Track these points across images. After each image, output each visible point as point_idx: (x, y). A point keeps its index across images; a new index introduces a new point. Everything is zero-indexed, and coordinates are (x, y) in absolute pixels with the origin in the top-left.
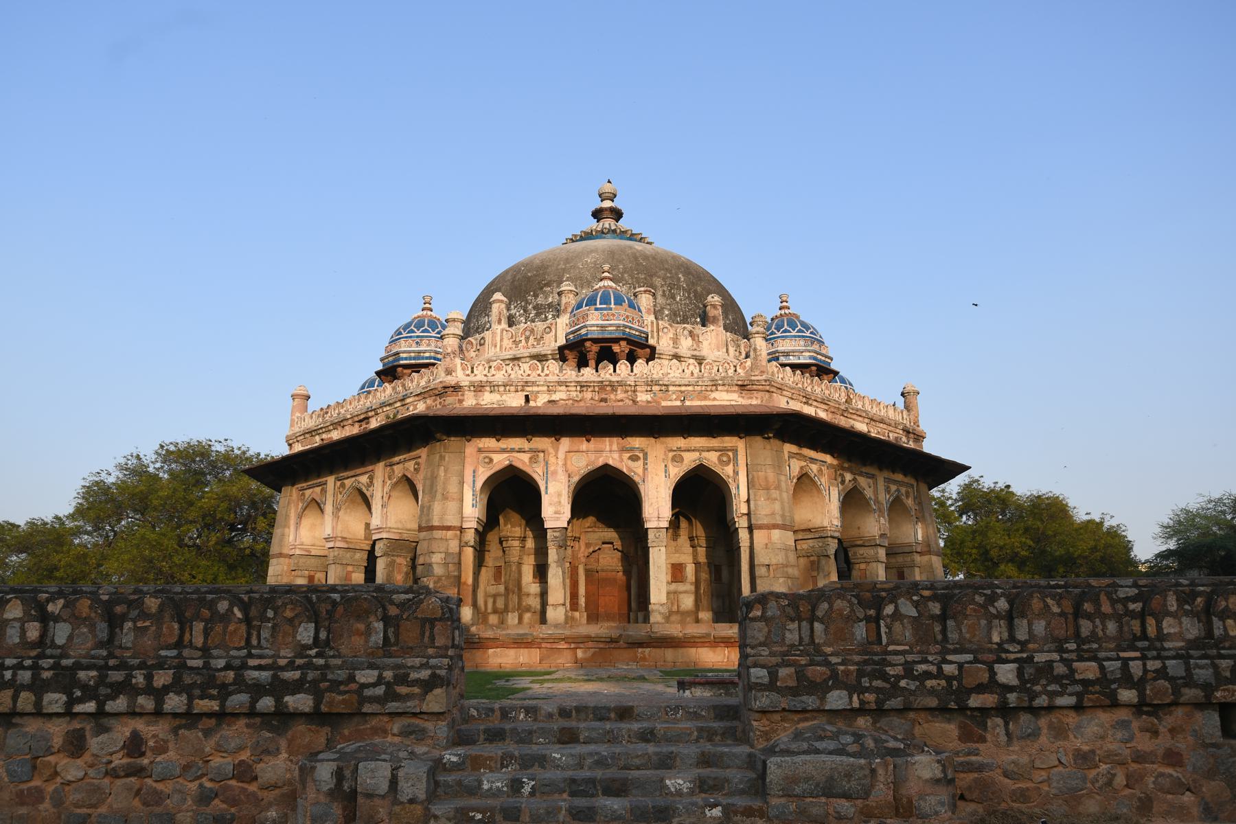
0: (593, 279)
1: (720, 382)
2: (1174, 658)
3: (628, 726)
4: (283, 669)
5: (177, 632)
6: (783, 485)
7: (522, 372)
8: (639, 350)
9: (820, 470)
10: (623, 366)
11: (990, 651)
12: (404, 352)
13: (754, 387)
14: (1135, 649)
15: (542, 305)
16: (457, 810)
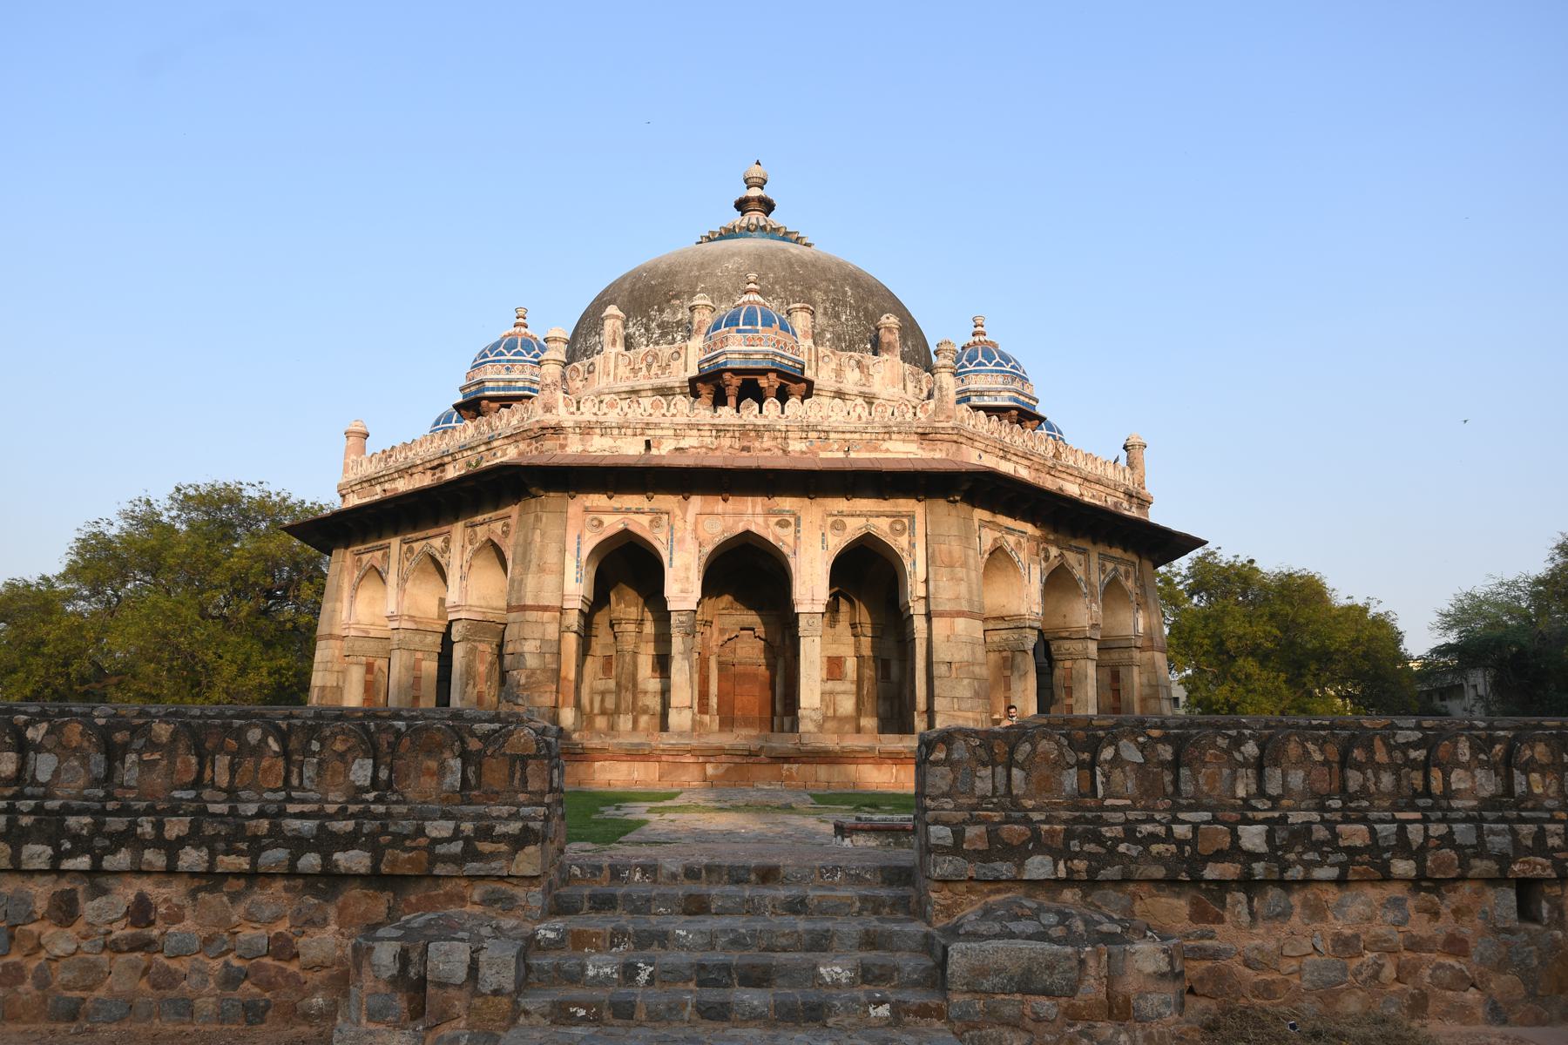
0: (735, 290)
1: (894, 429)
2: (1463, 821)
3: (773, 893)
4: (332, 817)
5: (194, 768)
6: (972, 561)
8: (792, 385)
9: (1019, 543)
10: (771, 405)
11: (1234, 808)
12: (491, 380)
13: (938, 436)
14: (1415, 809)
15: (668, 322)
16: (554, 1004)
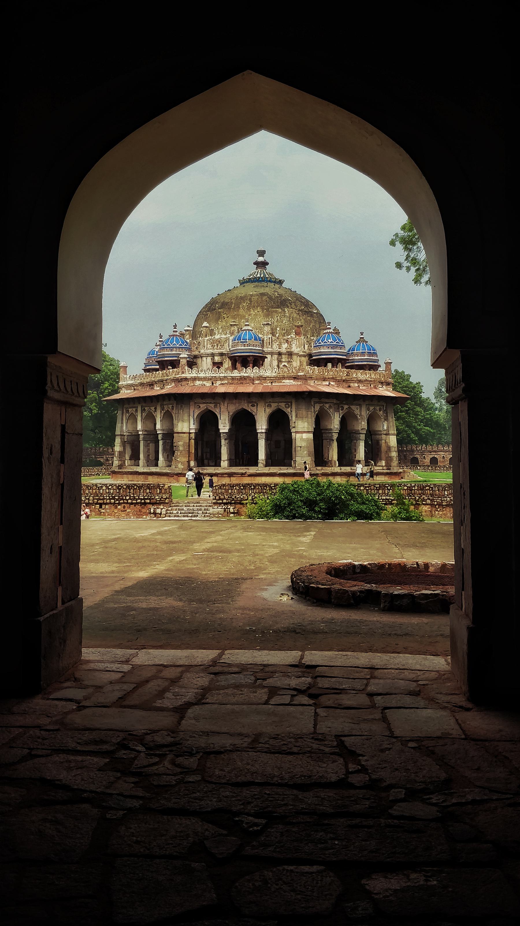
6: (309, 416)
7: (210, 372)
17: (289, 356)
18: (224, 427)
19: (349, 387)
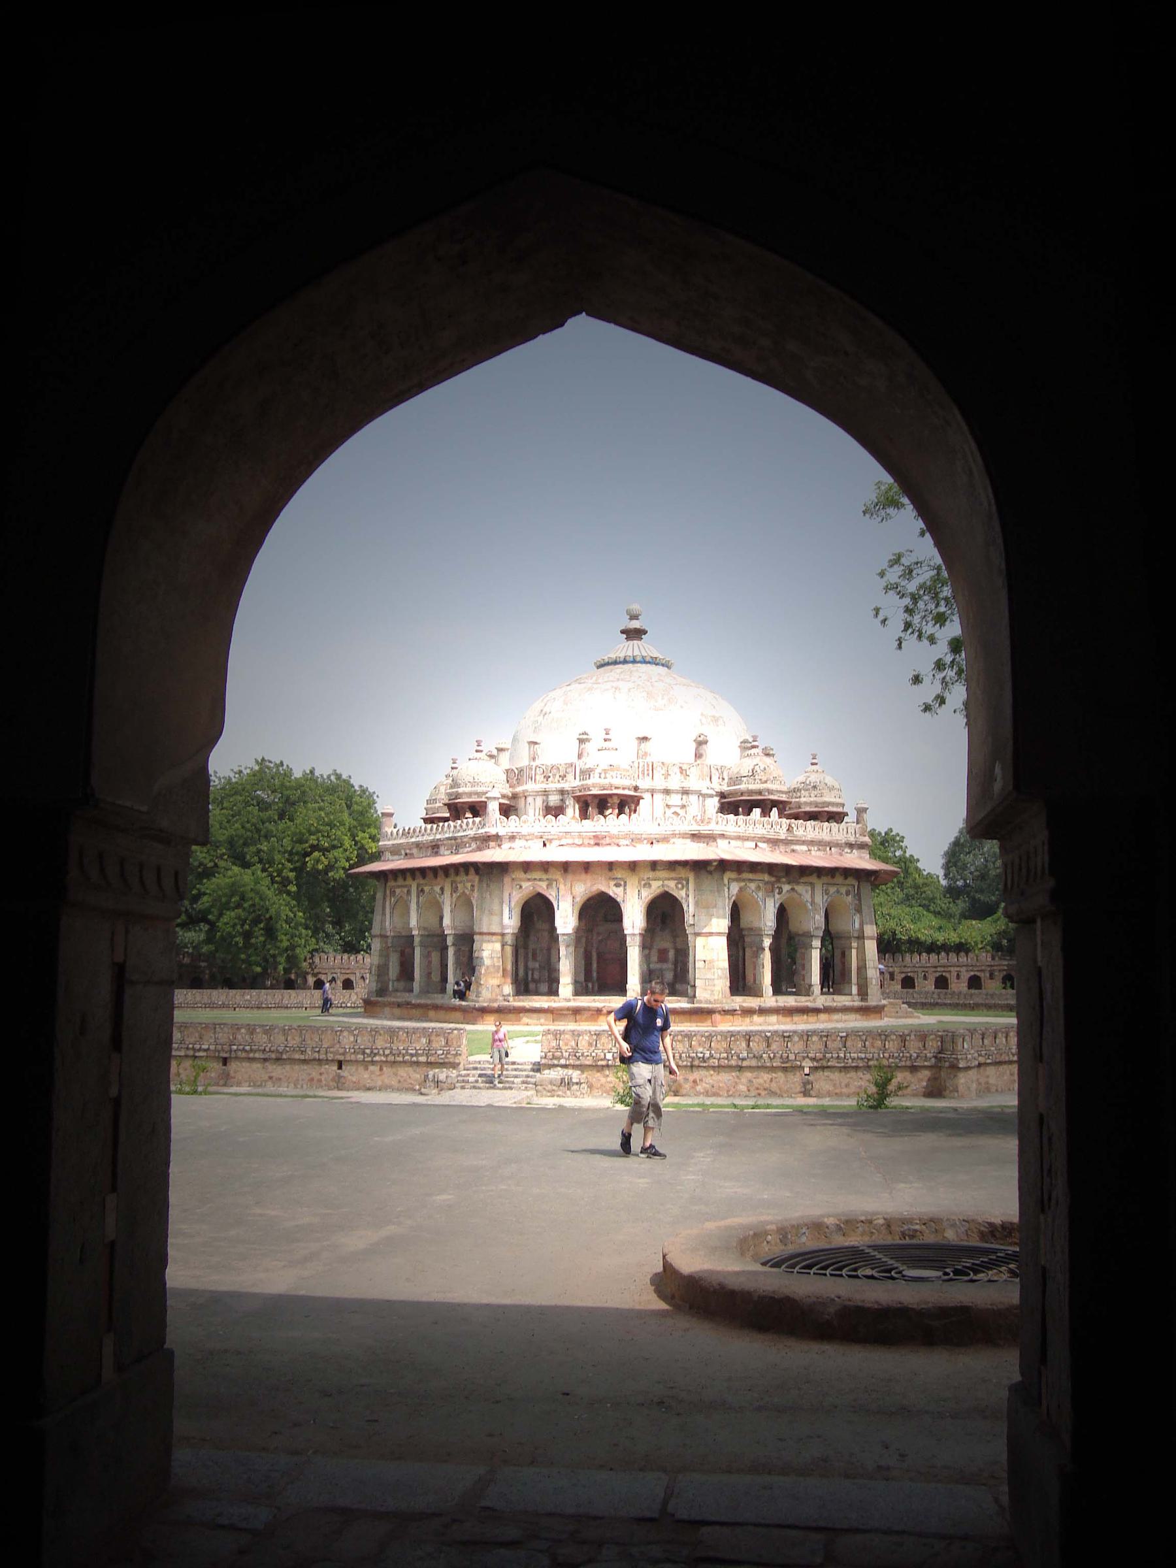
6: (720, 904)
9: (759, 888)
17: (684, 797)
18: (566, 921)
19: (793, 851)
